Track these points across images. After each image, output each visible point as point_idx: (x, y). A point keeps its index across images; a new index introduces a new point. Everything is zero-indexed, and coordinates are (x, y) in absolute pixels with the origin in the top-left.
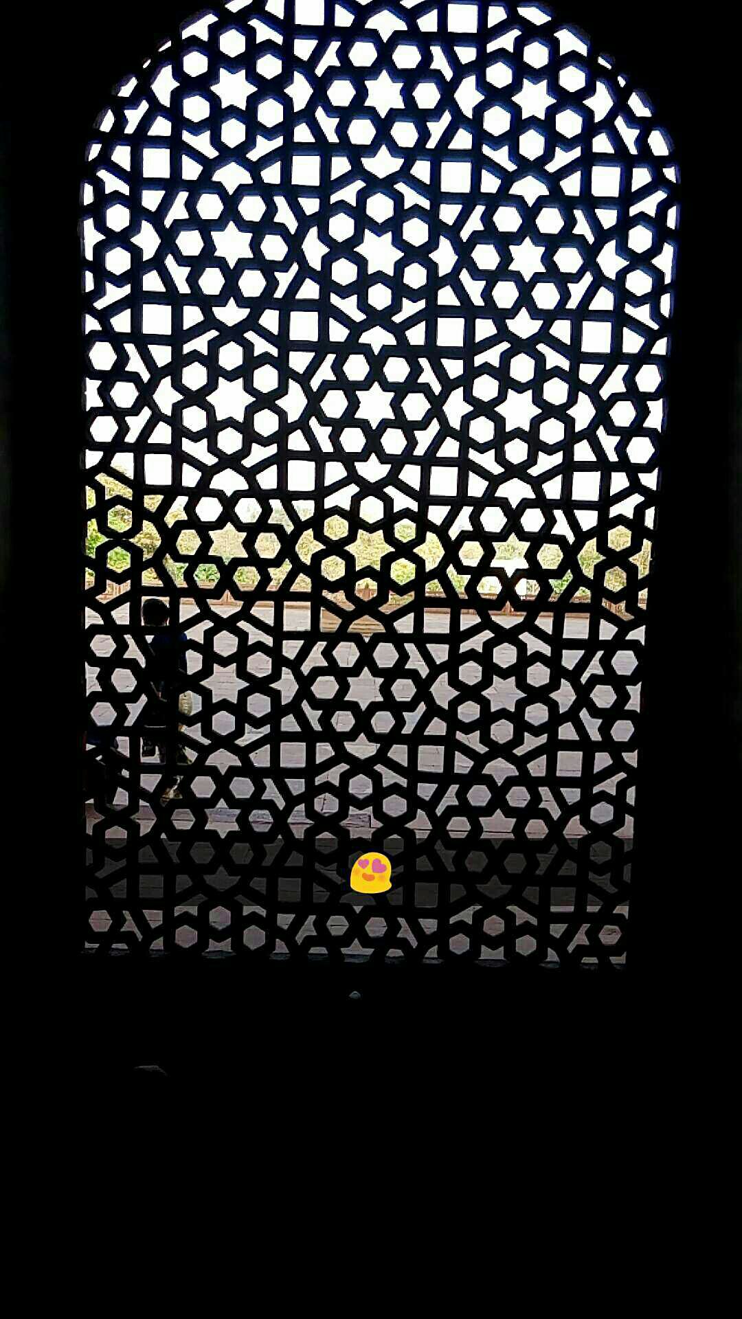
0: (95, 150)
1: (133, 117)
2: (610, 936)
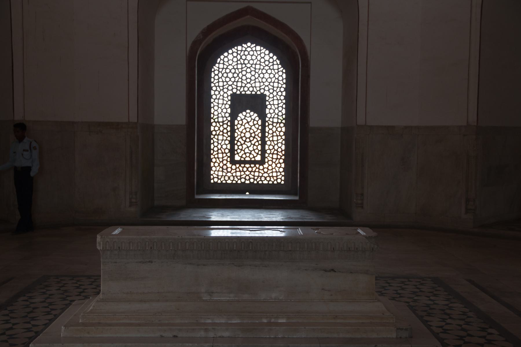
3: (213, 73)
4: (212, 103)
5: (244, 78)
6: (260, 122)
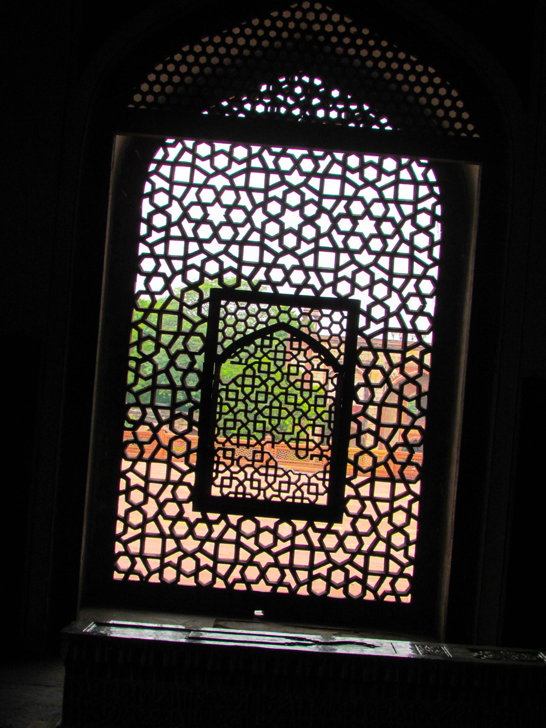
0: (153, 167)
1: (173, 153)
2: (403, 585)
3: (146, 202)
4: (135, 325)
5: (272, 229)
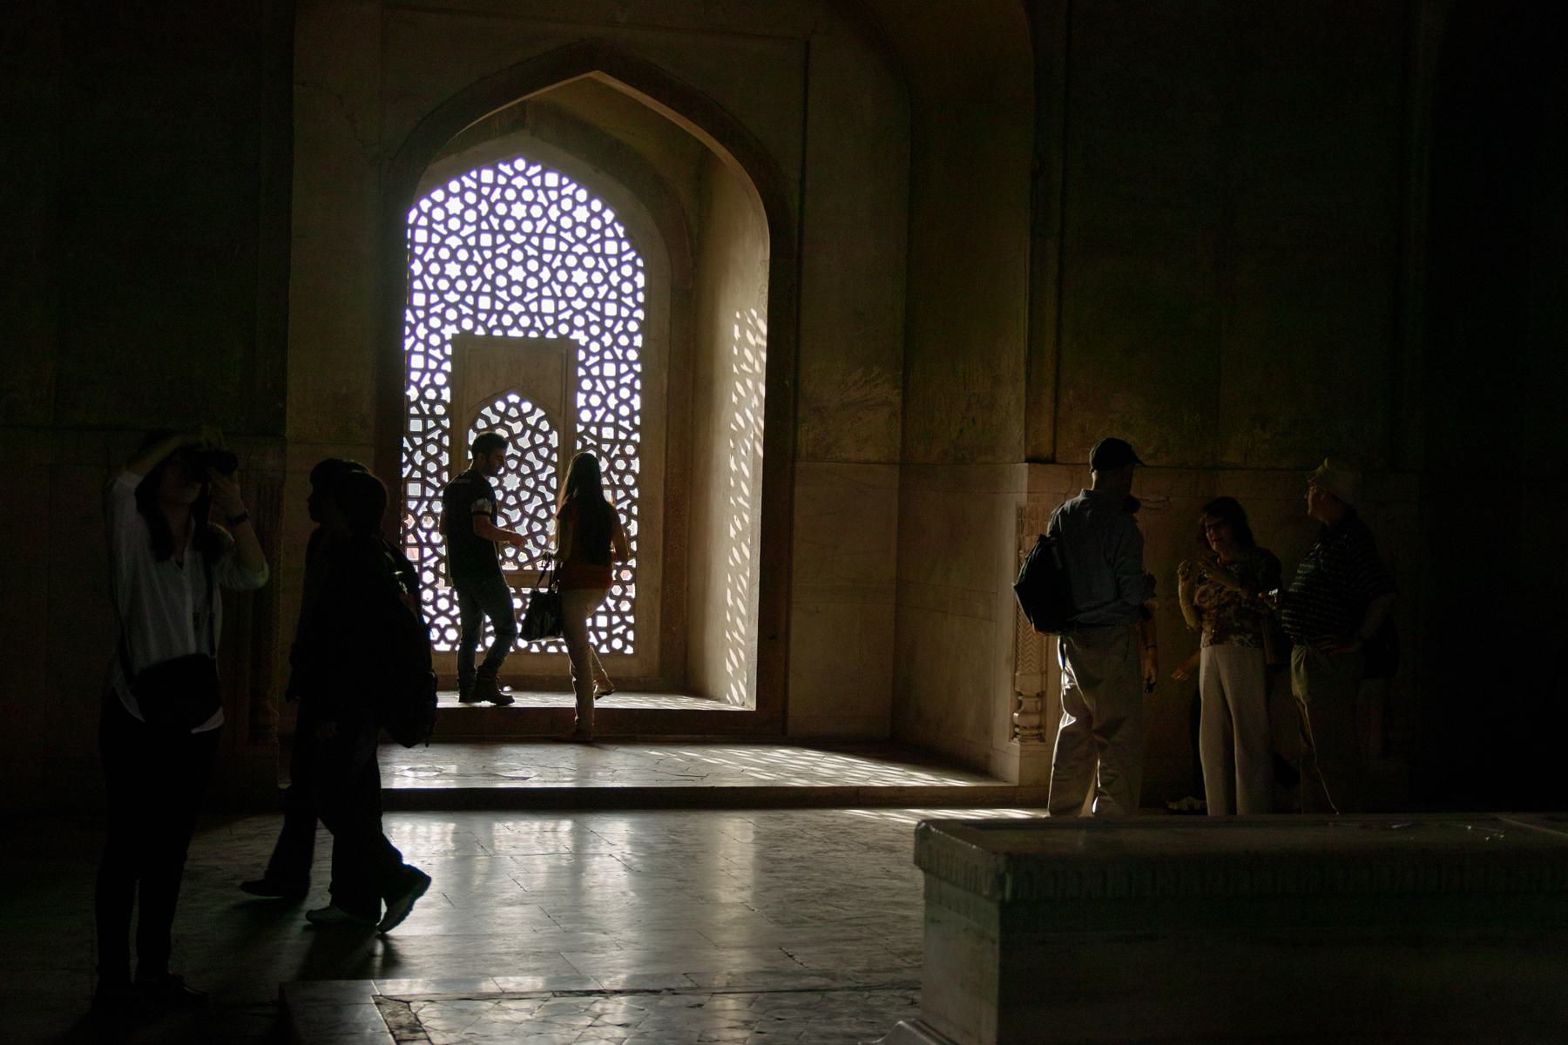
6: (554, 440)
